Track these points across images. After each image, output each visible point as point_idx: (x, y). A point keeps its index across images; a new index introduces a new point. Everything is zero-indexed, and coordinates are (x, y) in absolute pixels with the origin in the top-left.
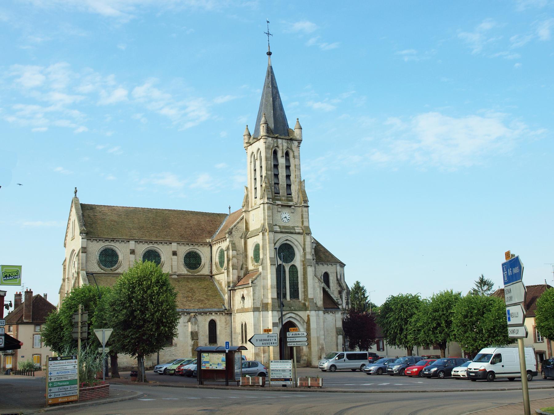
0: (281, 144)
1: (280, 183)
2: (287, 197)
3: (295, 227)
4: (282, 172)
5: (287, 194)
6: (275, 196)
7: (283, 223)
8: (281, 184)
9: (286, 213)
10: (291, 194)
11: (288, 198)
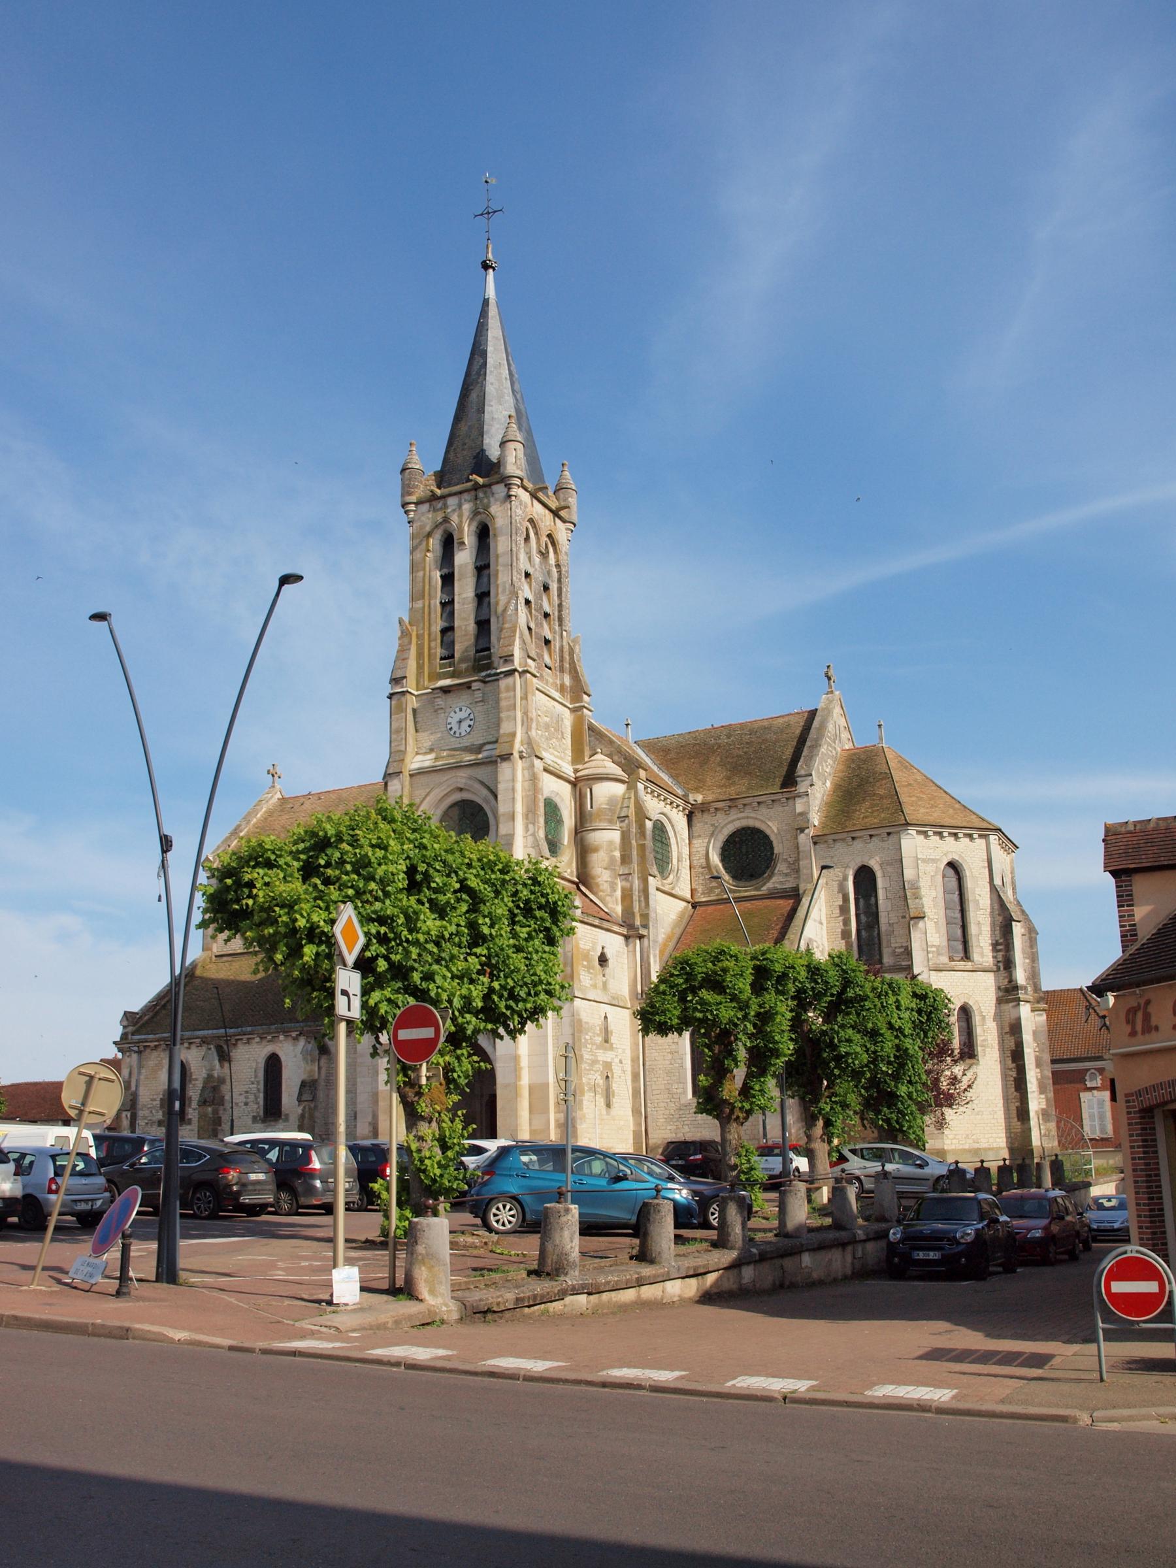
0: (454, 510)
1: (456, 624)
2: (476, 660)
3: (484, 744)
4: (465, 590)
5: (477, 651)
6: (442, 666)
7: (454, 739)
8: (460, 627)
9: (461, 710)
10: (488, 649)
11: (479, 661)
